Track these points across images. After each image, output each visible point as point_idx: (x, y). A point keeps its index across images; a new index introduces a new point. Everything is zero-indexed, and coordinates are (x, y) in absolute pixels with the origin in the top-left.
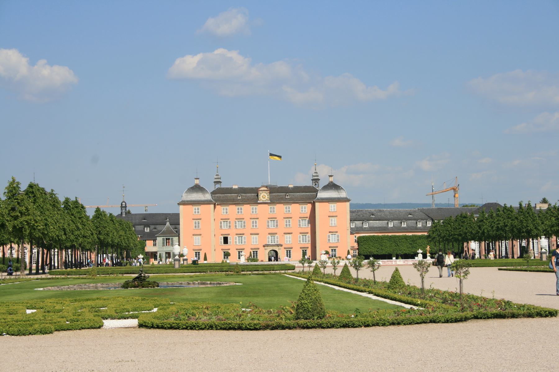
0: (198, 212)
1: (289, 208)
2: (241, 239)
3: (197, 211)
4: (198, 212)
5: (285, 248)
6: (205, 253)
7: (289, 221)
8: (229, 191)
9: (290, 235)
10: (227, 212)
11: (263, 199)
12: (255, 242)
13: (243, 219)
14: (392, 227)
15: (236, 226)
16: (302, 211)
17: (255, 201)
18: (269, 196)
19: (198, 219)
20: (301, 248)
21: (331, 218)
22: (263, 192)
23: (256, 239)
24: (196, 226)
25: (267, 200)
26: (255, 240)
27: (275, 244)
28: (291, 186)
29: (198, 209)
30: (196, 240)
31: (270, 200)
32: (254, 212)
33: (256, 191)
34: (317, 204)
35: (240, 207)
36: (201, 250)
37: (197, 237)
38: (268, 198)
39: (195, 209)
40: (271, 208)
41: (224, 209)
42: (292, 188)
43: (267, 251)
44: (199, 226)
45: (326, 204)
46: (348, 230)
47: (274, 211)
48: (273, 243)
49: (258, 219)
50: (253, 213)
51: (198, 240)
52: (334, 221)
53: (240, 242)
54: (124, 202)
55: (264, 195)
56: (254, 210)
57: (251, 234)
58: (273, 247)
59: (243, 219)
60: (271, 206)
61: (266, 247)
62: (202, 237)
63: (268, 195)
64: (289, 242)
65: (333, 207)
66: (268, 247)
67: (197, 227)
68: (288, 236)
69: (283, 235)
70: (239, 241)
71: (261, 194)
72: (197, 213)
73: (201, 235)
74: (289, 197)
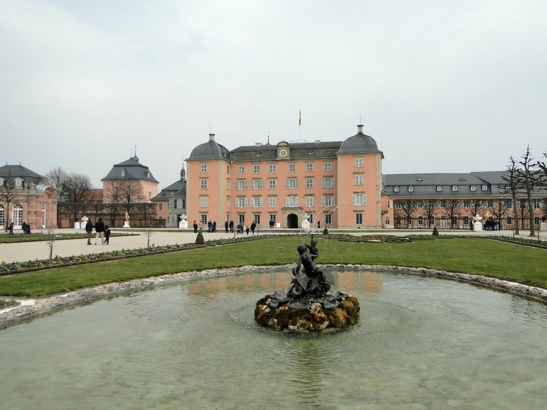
1: (311, 165)
2: (259, 201)
3: (204, 168)
4: (205, 170)
7: (311, 180)
11: (281, 156)
13: (260, 178)
15: (252, 187)
18: (289, 153)
19: (205, 178)
22: (282, 149)
23: (274, 201)
24: (202, 186)
25: (286, 156)
26: (273, 203)
27: (295, 207)
30: (202, 201)
31: (291, 156)
32: (273, 171)
35: (257, 165)
36: (207, 212)
37: (204, 198)
38: (288, 154)
39: (202, 167)
40: (291, 165)
41: (240, 168)
43: (286, 216)
44: (206, 185)
47: (294, 170)
48: (293, 207)
49: (276, 178)
50: (272, 172)
51: (205, 201)
53: (257, 205)
55: (284, 151)
56: (272, 169)
57: (269, 196)
58: (292, 210)
59: (260, 178)
60: (291, 164)
61: (285, 210)
63: (288, 152)
66: (288, 210)
67: (204, 186)
68: (310, 198)
69: (304, 198)
70: (256, 204)
71: (280, 150)
73: (207, 195)
74: (312, 153)
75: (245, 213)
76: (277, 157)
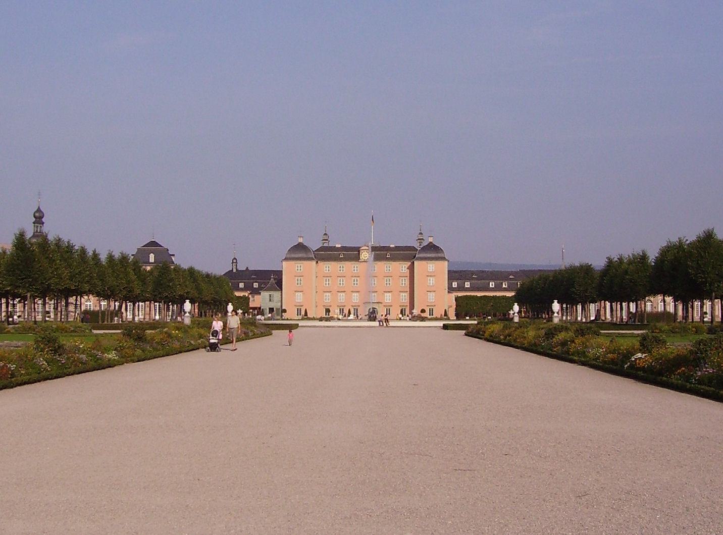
0: (300, 270)
5: (384, 306)
6: (306, 310)
8: (333, 249)
9: (390, 294)
10: (329, 270)
12: (356, 298)
14: (493, 288)
16: (402, 270)
17: (357, 258)
20: (400, 306)
21: (429, 278)
28: (392, 246)
29: (300, 267)
33: (358, 250)
34: (416, 263)
36: (302, 306)
42: (393, 248)
45: (424, 262)
52: (432, 281)
54: (235, 259)
62: (304, 294)
65: (431, 266)
69: (383, 294)
75: (330, 306)
76: (359, 259)
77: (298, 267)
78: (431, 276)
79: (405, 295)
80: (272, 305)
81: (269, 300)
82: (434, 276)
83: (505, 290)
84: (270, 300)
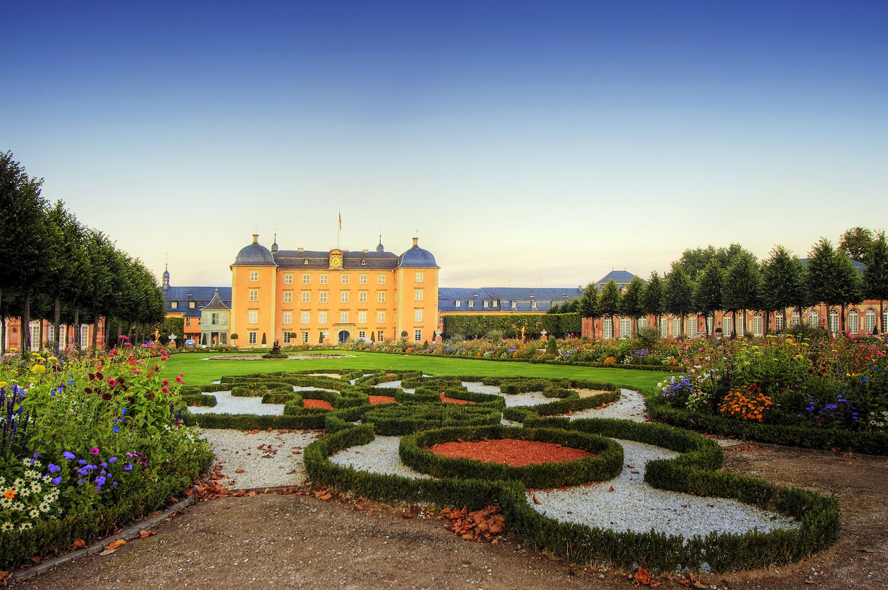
0: (256, 279)
3: (254, 277)
4: (256, 279)
5: (358, 328)
10: (290, 282)
12: (323, 318)
20: (377, 328)
21: (417, 290)
29: (256, 275)
36: (257, 329)
39: (252, 275)
41: (287, 276)
46: (436, 305)
47: (347, 281)
51: (255, 316)
52: (419, 295)
56: (324, 280)
64: (364, 321)
72: (254, 280)
76: (328, 266)
77: (252, 275)
78: (419, 288)
79: (383, 314)
80: (215, 328)
81: (211, 321)
82: (423, 288)
83: (471, 310)
84: (214, 323)
